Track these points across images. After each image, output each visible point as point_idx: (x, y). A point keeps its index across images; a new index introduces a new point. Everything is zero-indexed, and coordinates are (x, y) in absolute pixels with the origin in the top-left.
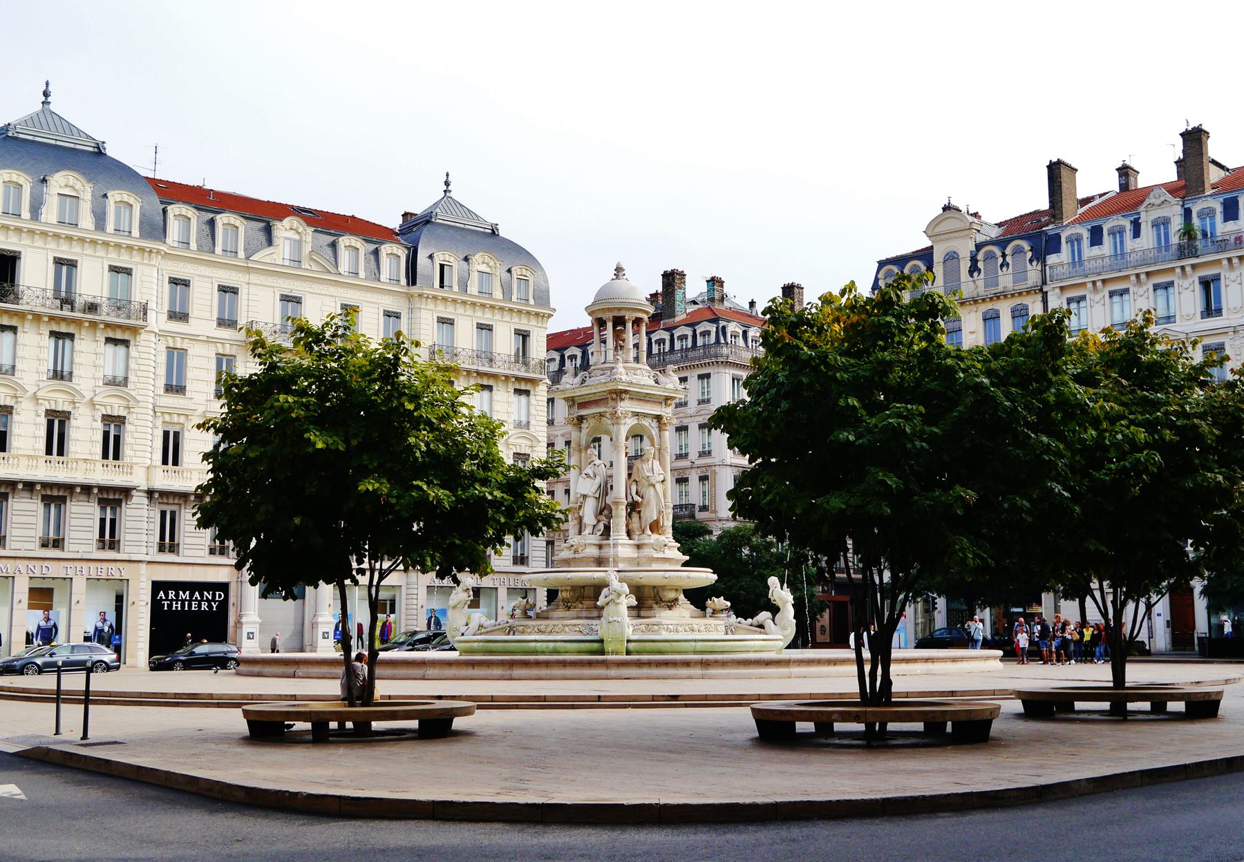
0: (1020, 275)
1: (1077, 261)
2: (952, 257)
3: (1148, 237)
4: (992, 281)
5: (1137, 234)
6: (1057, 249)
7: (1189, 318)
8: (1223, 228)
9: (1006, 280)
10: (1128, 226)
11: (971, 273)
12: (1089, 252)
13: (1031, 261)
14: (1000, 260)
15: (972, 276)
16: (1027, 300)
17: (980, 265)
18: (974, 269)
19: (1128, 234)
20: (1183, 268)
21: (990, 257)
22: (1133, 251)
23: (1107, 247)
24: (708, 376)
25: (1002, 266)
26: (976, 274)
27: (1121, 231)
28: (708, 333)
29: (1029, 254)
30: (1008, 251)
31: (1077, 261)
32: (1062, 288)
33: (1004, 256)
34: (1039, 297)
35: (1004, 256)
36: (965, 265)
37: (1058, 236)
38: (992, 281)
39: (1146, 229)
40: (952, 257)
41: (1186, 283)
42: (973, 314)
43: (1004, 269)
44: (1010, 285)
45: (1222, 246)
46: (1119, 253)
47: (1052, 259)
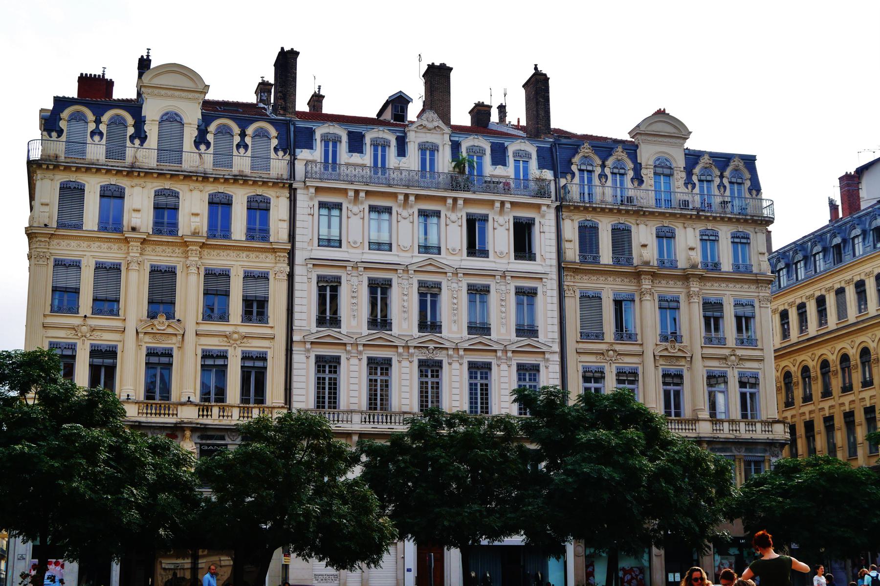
0: (261, 161)
1: (330, 162)
2: (171, 119)
3: (412, 160)
4: (223, 158)
5: (402, 151)
6: (309, 145)
8: (489, 170)
9: (242, 163)
10: (393, 140)
11: (197, 144)
12: (344, 155)
13: (276, 150)
14: (237, 139)
15: (197, 147)
16: (268, 192)
17: (210, 137)
18: (201, 140)
19: (392, 151)
20: (455, 200)
21: (224, 131)
23: (366, 158)
25: (238, 146)
27: (385, 145)
29: (274, 142)
30: (250, 130)
31: (330, 162)
32: (317, 189)
33: (243, 135)
34: (286, 193)
35: (243, 135)
36: (190, 134)
37: (312, 132)
38: (223, 158)
39: (412, 149)
40: (171, 119)
41: (453, 216)
42: (196, 193)
43: (242, 150)
44: (247, 171)
45: (491, 185)
46: (379, 166)
47: (303, 154)
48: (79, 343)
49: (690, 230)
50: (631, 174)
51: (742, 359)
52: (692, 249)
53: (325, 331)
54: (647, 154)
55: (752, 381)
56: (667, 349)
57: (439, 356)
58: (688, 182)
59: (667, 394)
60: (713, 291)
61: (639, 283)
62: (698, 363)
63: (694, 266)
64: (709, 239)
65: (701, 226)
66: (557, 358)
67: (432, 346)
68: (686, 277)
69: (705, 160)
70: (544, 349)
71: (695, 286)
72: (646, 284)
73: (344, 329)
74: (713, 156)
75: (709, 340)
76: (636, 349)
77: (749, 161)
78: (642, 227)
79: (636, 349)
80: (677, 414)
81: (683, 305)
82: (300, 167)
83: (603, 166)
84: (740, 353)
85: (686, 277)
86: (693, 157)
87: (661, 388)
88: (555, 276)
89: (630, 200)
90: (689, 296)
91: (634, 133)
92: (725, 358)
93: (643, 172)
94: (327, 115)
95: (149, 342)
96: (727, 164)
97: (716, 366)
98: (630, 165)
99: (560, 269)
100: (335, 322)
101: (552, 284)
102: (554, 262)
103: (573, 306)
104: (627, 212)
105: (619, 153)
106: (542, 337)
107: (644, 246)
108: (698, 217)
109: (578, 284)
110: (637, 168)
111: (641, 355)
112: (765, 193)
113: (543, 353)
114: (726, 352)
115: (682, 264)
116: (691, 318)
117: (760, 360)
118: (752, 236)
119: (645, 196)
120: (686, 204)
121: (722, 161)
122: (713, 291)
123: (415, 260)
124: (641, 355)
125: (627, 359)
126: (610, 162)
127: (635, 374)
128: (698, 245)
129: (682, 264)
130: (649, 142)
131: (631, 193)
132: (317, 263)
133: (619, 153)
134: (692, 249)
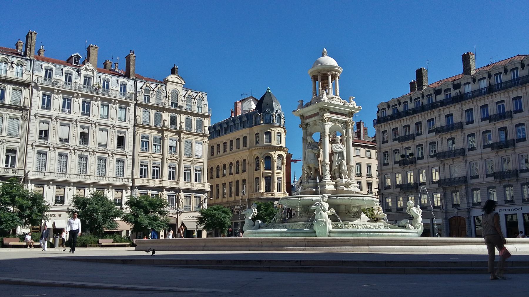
53: (42, 141)
55: (199, 169)
56: (171, 157)
57: (87, 154)
66: (131, 157)
67: (84, 150)
70: (127, 154)
73: (49, 141)
88: (133, 128)
89: (162, 104)
99: (135, 126)
101: (131, 130)
102: (133, 123)
103: (139, 140)
106: (126, 150)
109: (141, 132)
113: (126, 155)
114: (192, 159)
123: (79, 118)
125: (156, 159)
130: (170, 84)
131: (162, 101)
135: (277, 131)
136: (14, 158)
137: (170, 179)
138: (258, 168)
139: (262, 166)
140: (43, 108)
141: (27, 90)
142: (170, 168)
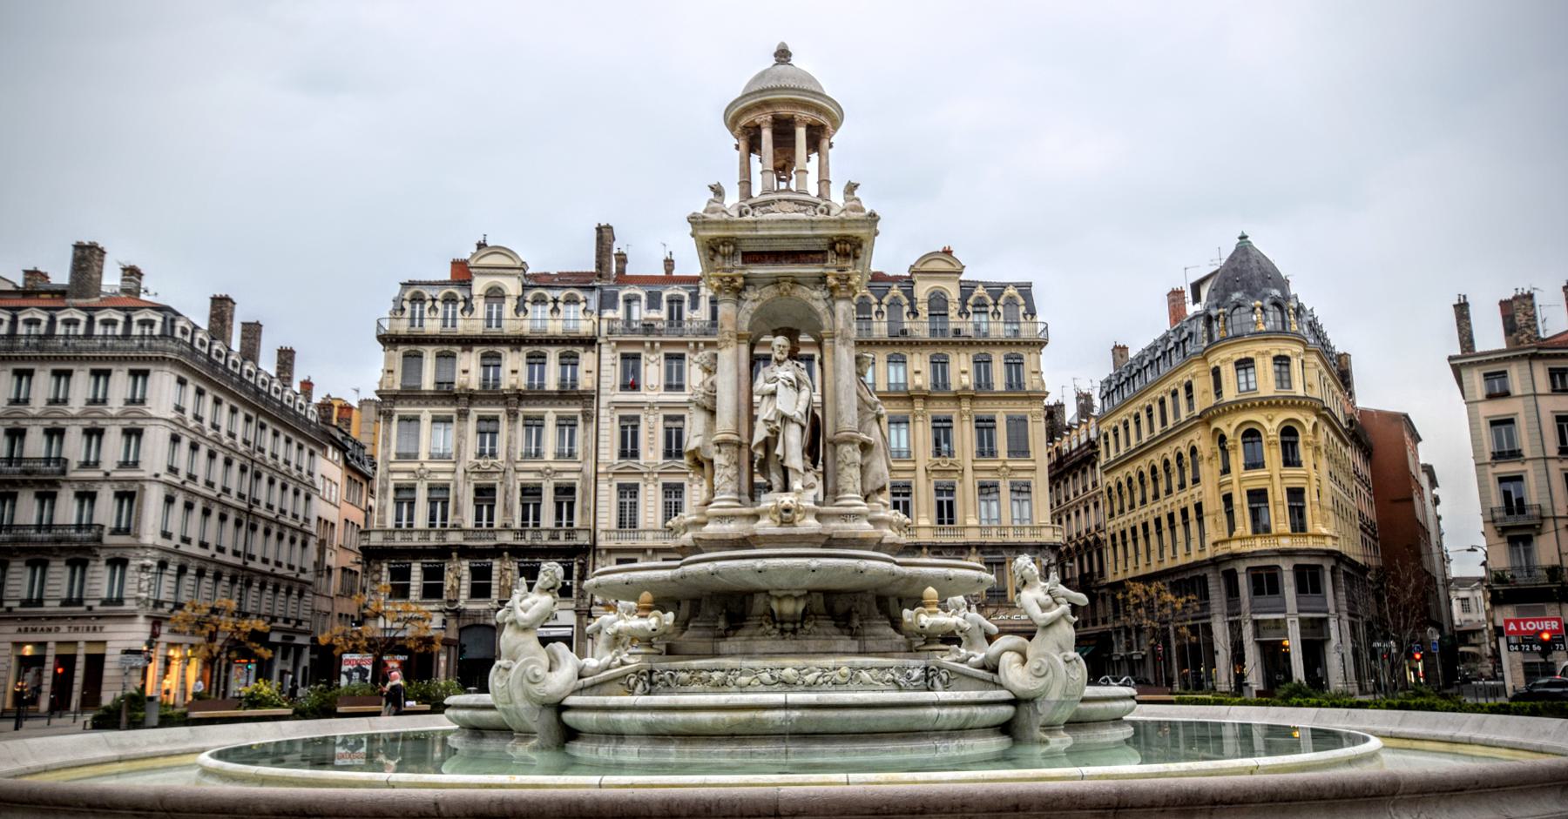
5: (695, 305)
6: (614, 306)
7: (651, 388)
11: (517, 311)
22: (691, 320)
24: (145, 374)
26: (522, 314)
28: (151, 323)
32: (619, 343)
37: (616, 294)
47: (608, 314)
48: (418, 484)
49: (963, 357)
50: (906, 309)
51: (1012, 470)
52: (964, 372)
53: (625, 462)
54: (922, 290)
58: (963, 312)
59: (940, 504)
60: (984, 409)
61: (913, 407)
62: (969, 474)
63: (965, 388)
64: (982, 363)
65: (974, 352)
68: (957, 398)
69: (980, 291)
71: (966, 406)
72: (919, 406)
73: (642, 461)
74: (986, 285)
75: (981, 453)
76: (911, 465)
77: (1025, 290)
78: (916, 356)
79: (911, 465)
80: (951, 522)
81: (955, 424)
82: (604, 325)
83: (880, 303)
84: (1010, 464)
85: (957, 398)
86: (967, 289)
87: (933, 499)
89: (904, 332)
90: (961, 416)
91: (914, 270)
92: (997, 470)
93: (918, 306)
94: (632, 277)
95: (476, 479)
96: (1001, 293)
97: (987, 477)
98: (905, 301)
100: (635, 455)
104: (901, 343)
105: (895, 290)
107: (918, 373)
108: (970, 344)
110: (912, 304)
111: (914, 470)
112: (1039, 318)
114: (998, 464)
115: (954, 386)
116: (964, 436)
117: (1033, 470)
118: (1026, 357)
119: (920, 328)
120: (957, 332)
121: (996, 290)
122: (984, 409)
124: (914, 470)
125: (900, 475)
126: (886, 300)
127: (908, 486)
128: (971, 368)
129: (954, 386)
131: (906, 326)
132: (618, 406)
133: (895, 290)
134: (964, 372)
135: (1275, 353)
136: (571, 505)
137: (941, 522)
138: (1226, 470)
139: (1237, 460)
140: (669, 387)
141: (589, 354)
142: (939, 492)
